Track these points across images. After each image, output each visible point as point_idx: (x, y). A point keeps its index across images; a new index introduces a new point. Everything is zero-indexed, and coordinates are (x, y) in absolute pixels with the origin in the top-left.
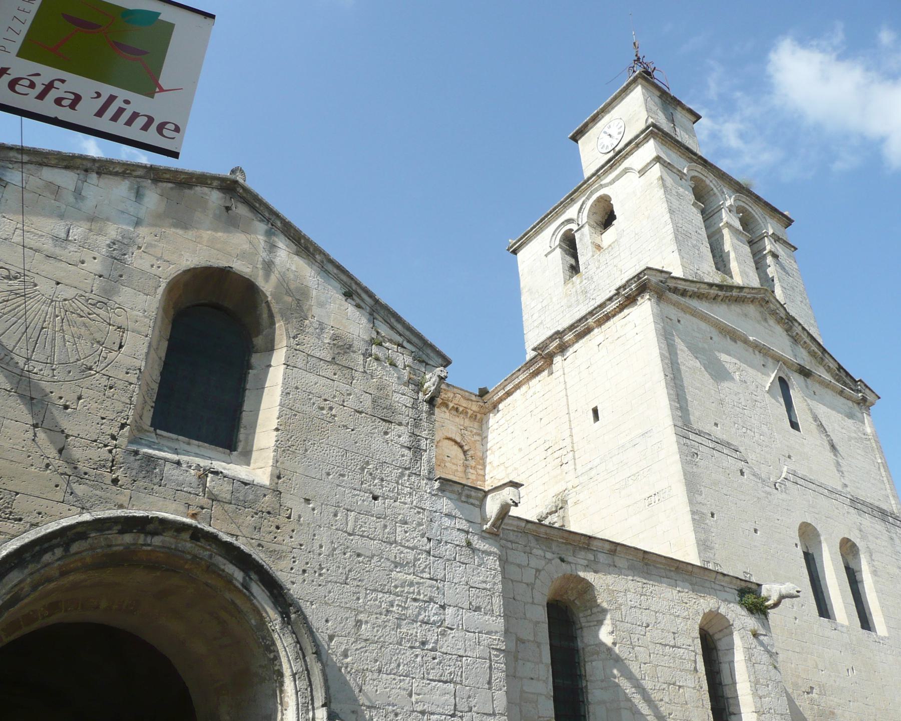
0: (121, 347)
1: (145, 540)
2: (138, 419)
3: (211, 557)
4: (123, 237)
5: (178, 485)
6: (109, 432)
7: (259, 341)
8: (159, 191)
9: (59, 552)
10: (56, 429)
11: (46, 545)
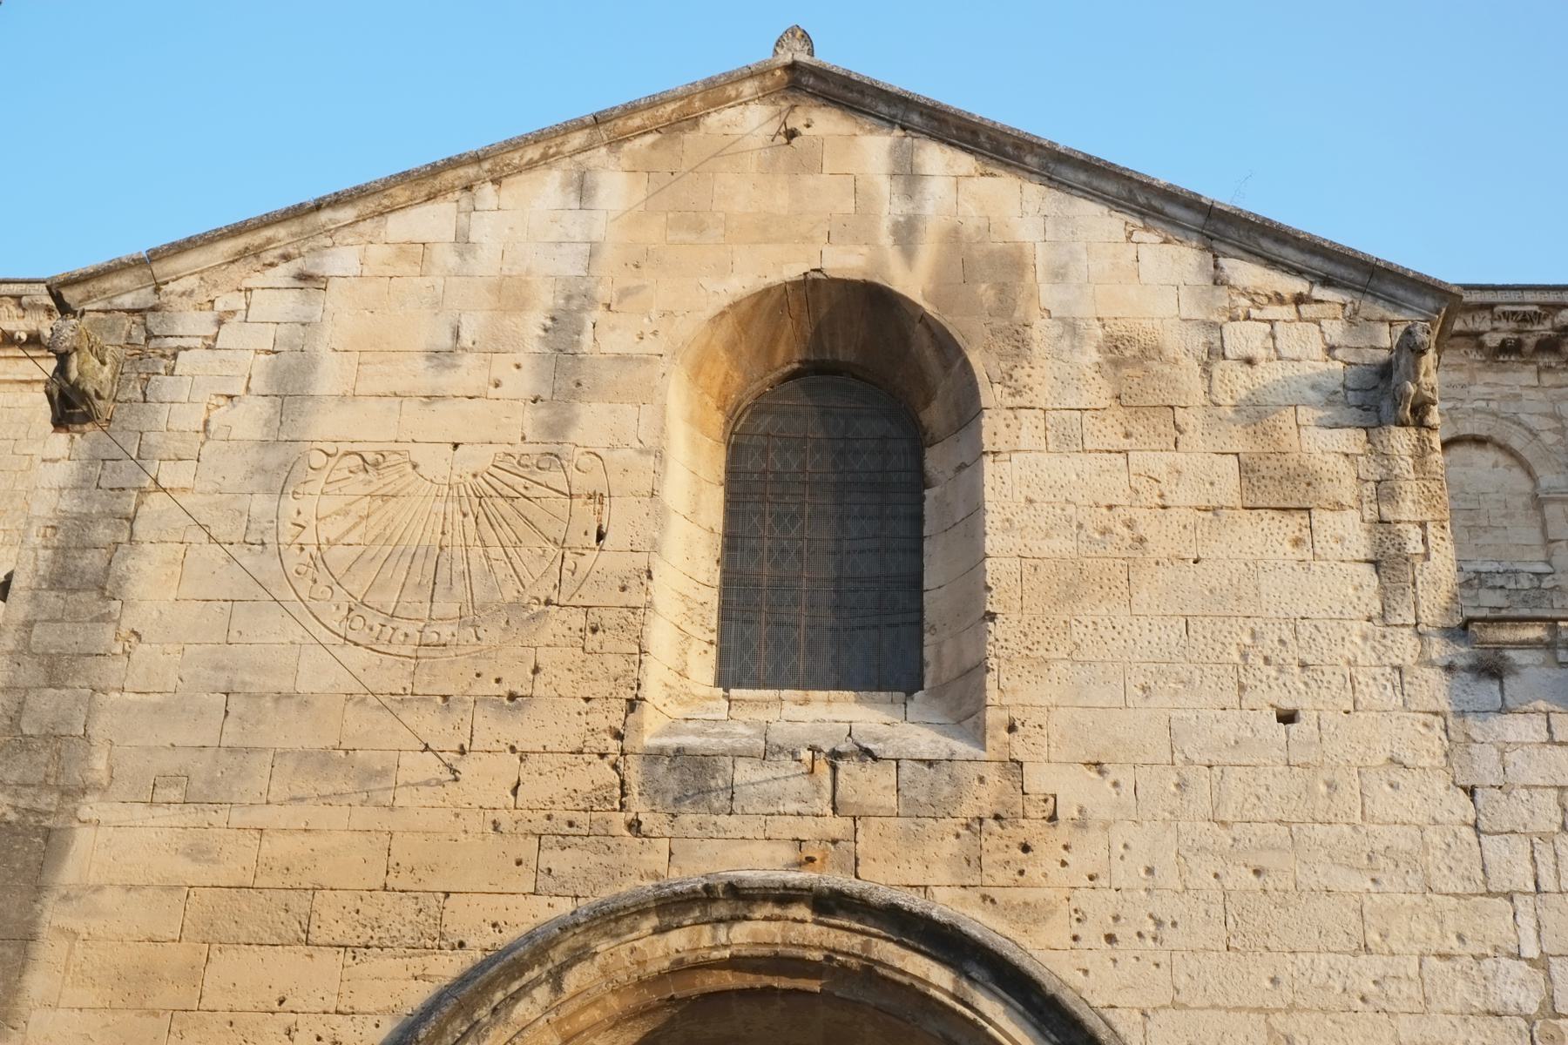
0: (600, 536)
1: (714, 938)
2: (672, 679)
3: (866, 946)
4: (569, 298)
5: (769, 803)
6: (605, 725)
7: (934, 416)
8: (625, 163)
9: (542, 994)
10: (495, 746)
11: (515, 986)
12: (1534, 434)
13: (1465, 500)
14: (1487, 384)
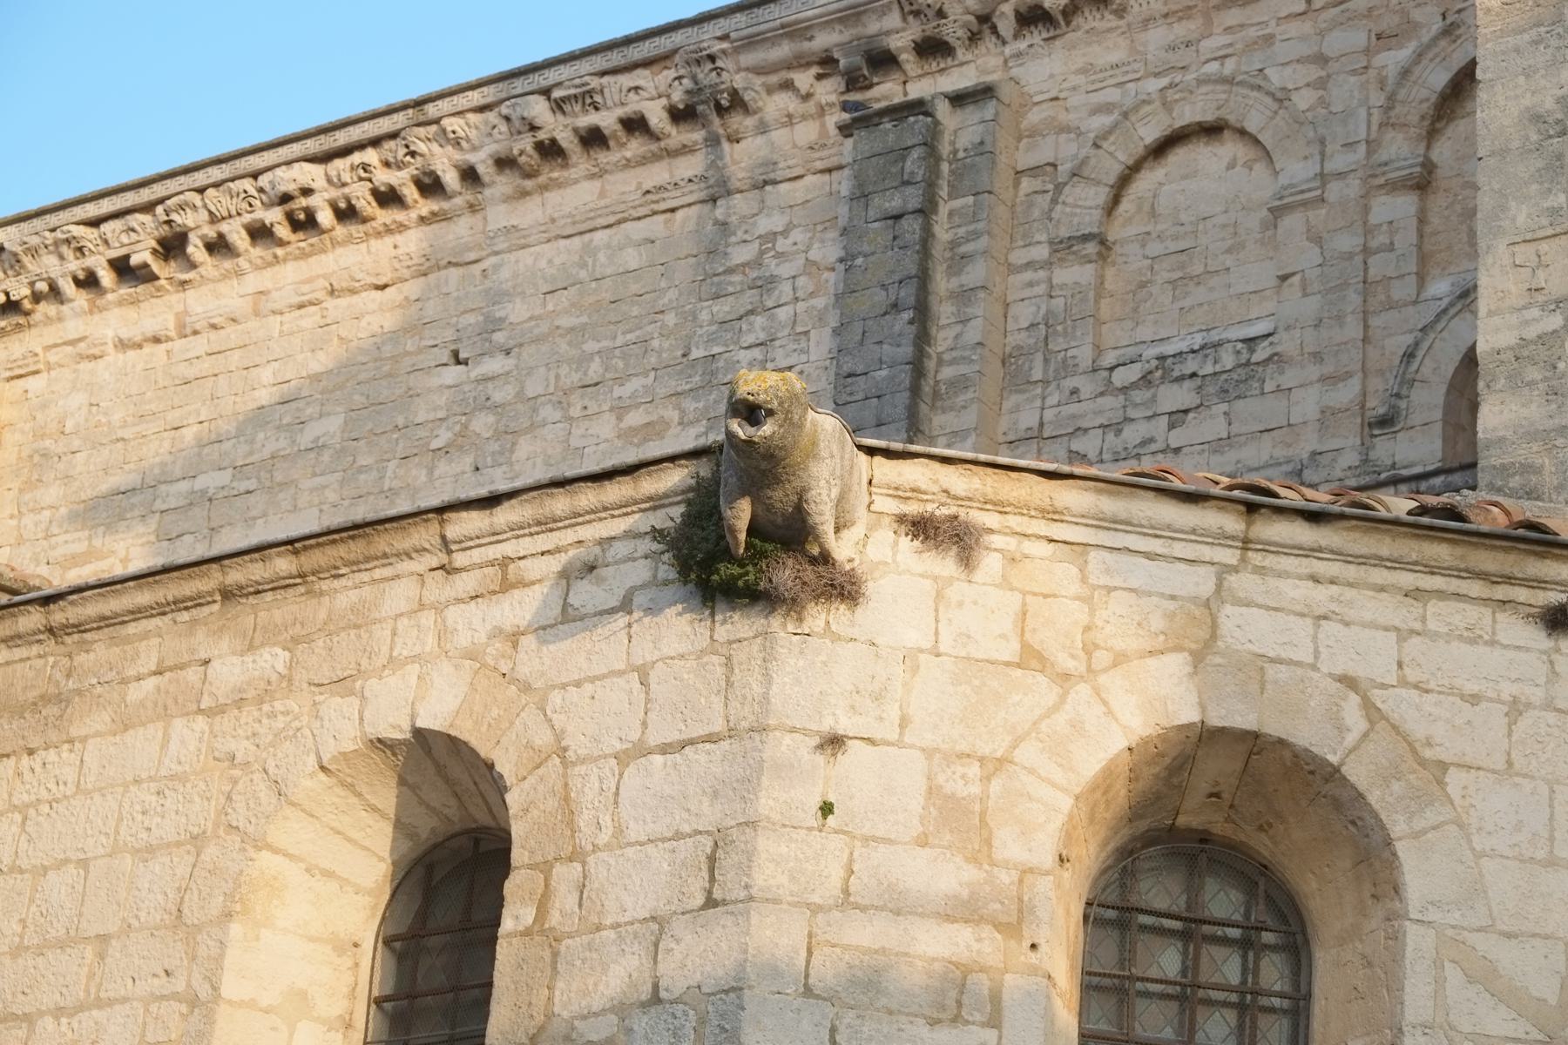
12: (1281, 98)
13: (1176, 238)
14: (1228, 30)
